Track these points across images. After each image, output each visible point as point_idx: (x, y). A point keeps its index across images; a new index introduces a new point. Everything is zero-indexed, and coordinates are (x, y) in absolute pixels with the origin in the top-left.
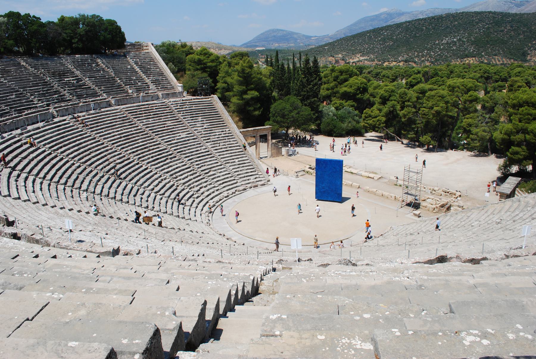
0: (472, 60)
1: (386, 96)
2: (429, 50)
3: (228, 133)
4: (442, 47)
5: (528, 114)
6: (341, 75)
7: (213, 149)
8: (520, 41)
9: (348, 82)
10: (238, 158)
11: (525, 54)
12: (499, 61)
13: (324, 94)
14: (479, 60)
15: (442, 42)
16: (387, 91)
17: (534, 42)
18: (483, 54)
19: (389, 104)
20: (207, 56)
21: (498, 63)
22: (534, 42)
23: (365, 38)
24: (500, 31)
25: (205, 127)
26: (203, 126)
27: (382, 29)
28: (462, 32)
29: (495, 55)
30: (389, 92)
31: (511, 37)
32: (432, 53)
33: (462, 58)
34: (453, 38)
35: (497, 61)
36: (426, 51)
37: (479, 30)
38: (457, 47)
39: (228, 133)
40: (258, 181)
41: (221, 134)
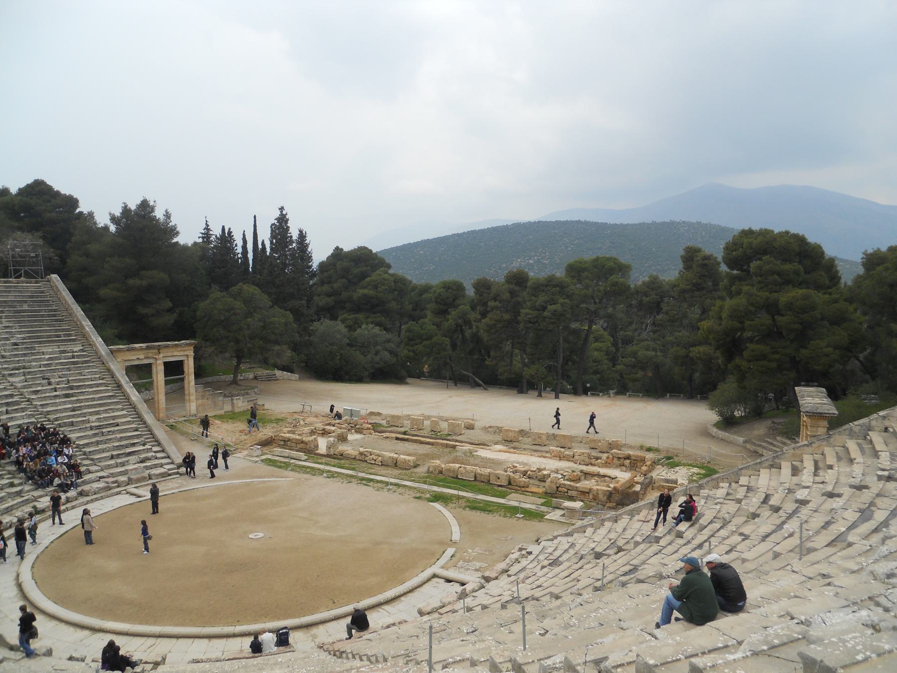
1: (448, 298)
3: (78, 356)
5: (774, 273)
7: (25, 390)
9: (368, 279)
10: (97, 413)
13: (321, 304)
17: (647, 265)
19: (453, 313)
22: (647, 265)
26: (7, 339)
28: (540, 250)
34: (527, 260)
38: (534, 272)
39: (78, 356)
40: (150, 468)
41: (56, 358)
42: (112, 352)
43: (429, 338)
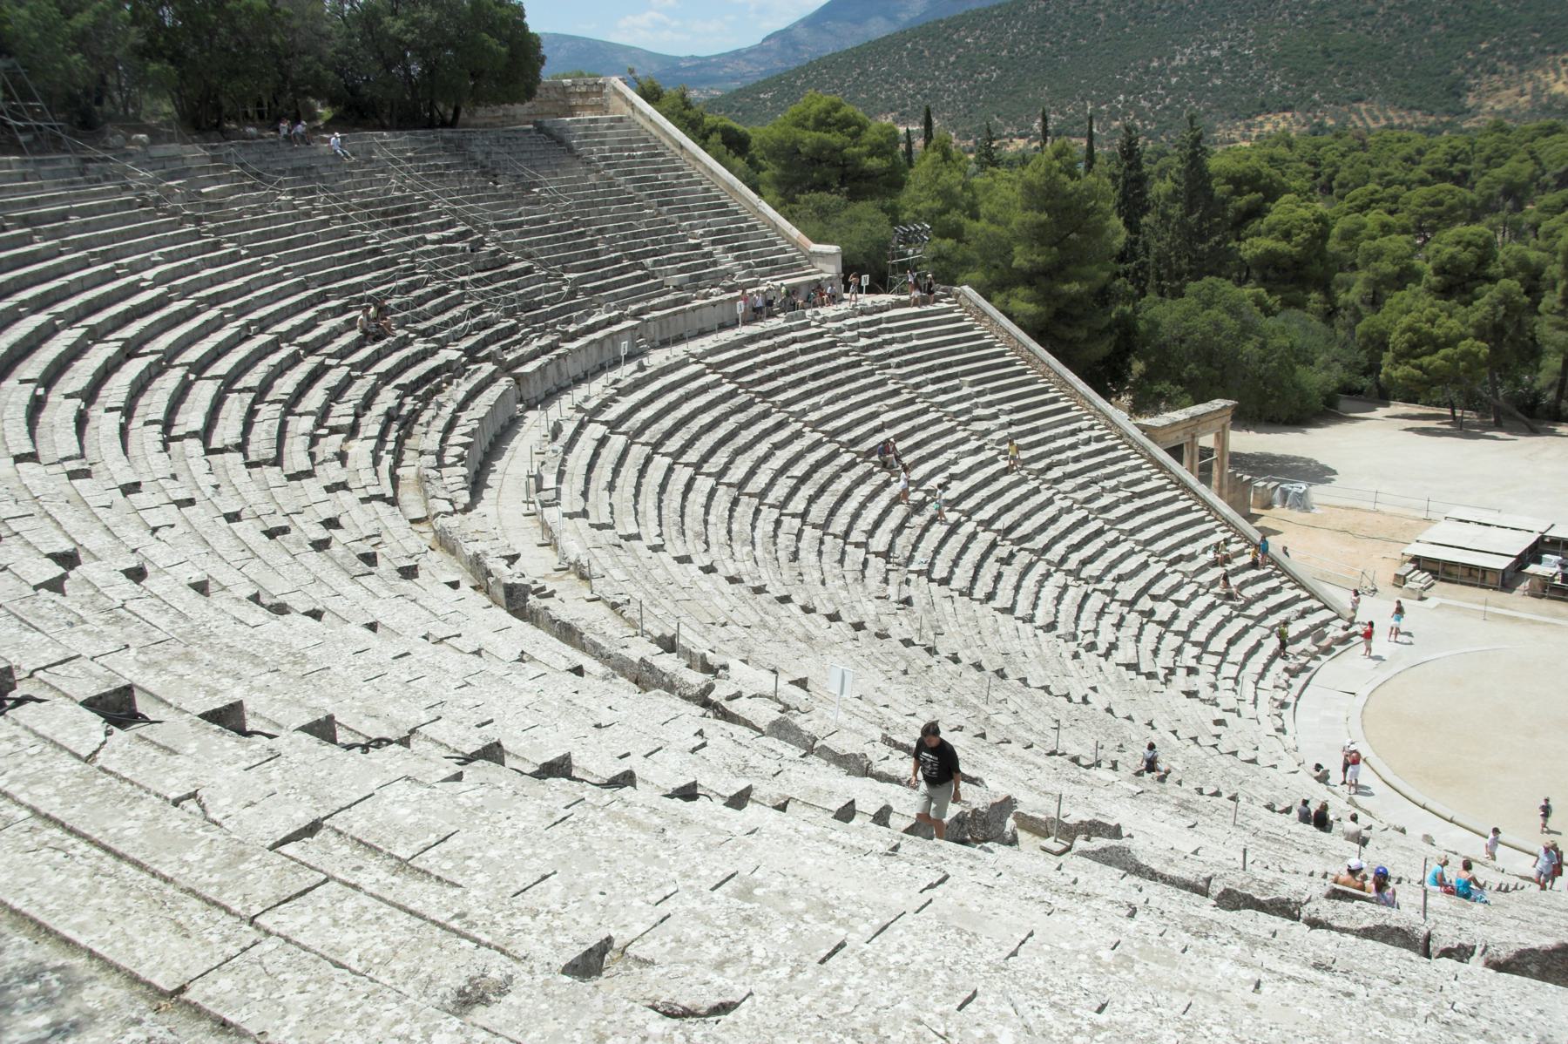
0: (1284, 119)
2: (1131, 93)
4: (1174, 80)
6: (1238, 192)
8: (1435, 45)
10: (1194, 539)
11: (1456, 90)
12: (1375, 119)
14: (1308, 121)
15: (1174, 64)
16: (1469, 244)
17: (1483, 46)
18: (1316, 96)
20: (853, 129)
21: (1373, 125)
22: (1483, 46)
23: (901, 57)
24: (1364, 15)
25: (1004, 419)
27: (956, 24)
28: (1233, 25)
29: (1360, 100)
30: (1477, 246)
31: (1403, 31)
32: (1143, 103)
33: (1249, 117)
35: (1369, 121)
36: (1121, 98)
37: (1291, 14)
38: (1224, 78)
42: (1144, 429)
43: (1451, 342)
